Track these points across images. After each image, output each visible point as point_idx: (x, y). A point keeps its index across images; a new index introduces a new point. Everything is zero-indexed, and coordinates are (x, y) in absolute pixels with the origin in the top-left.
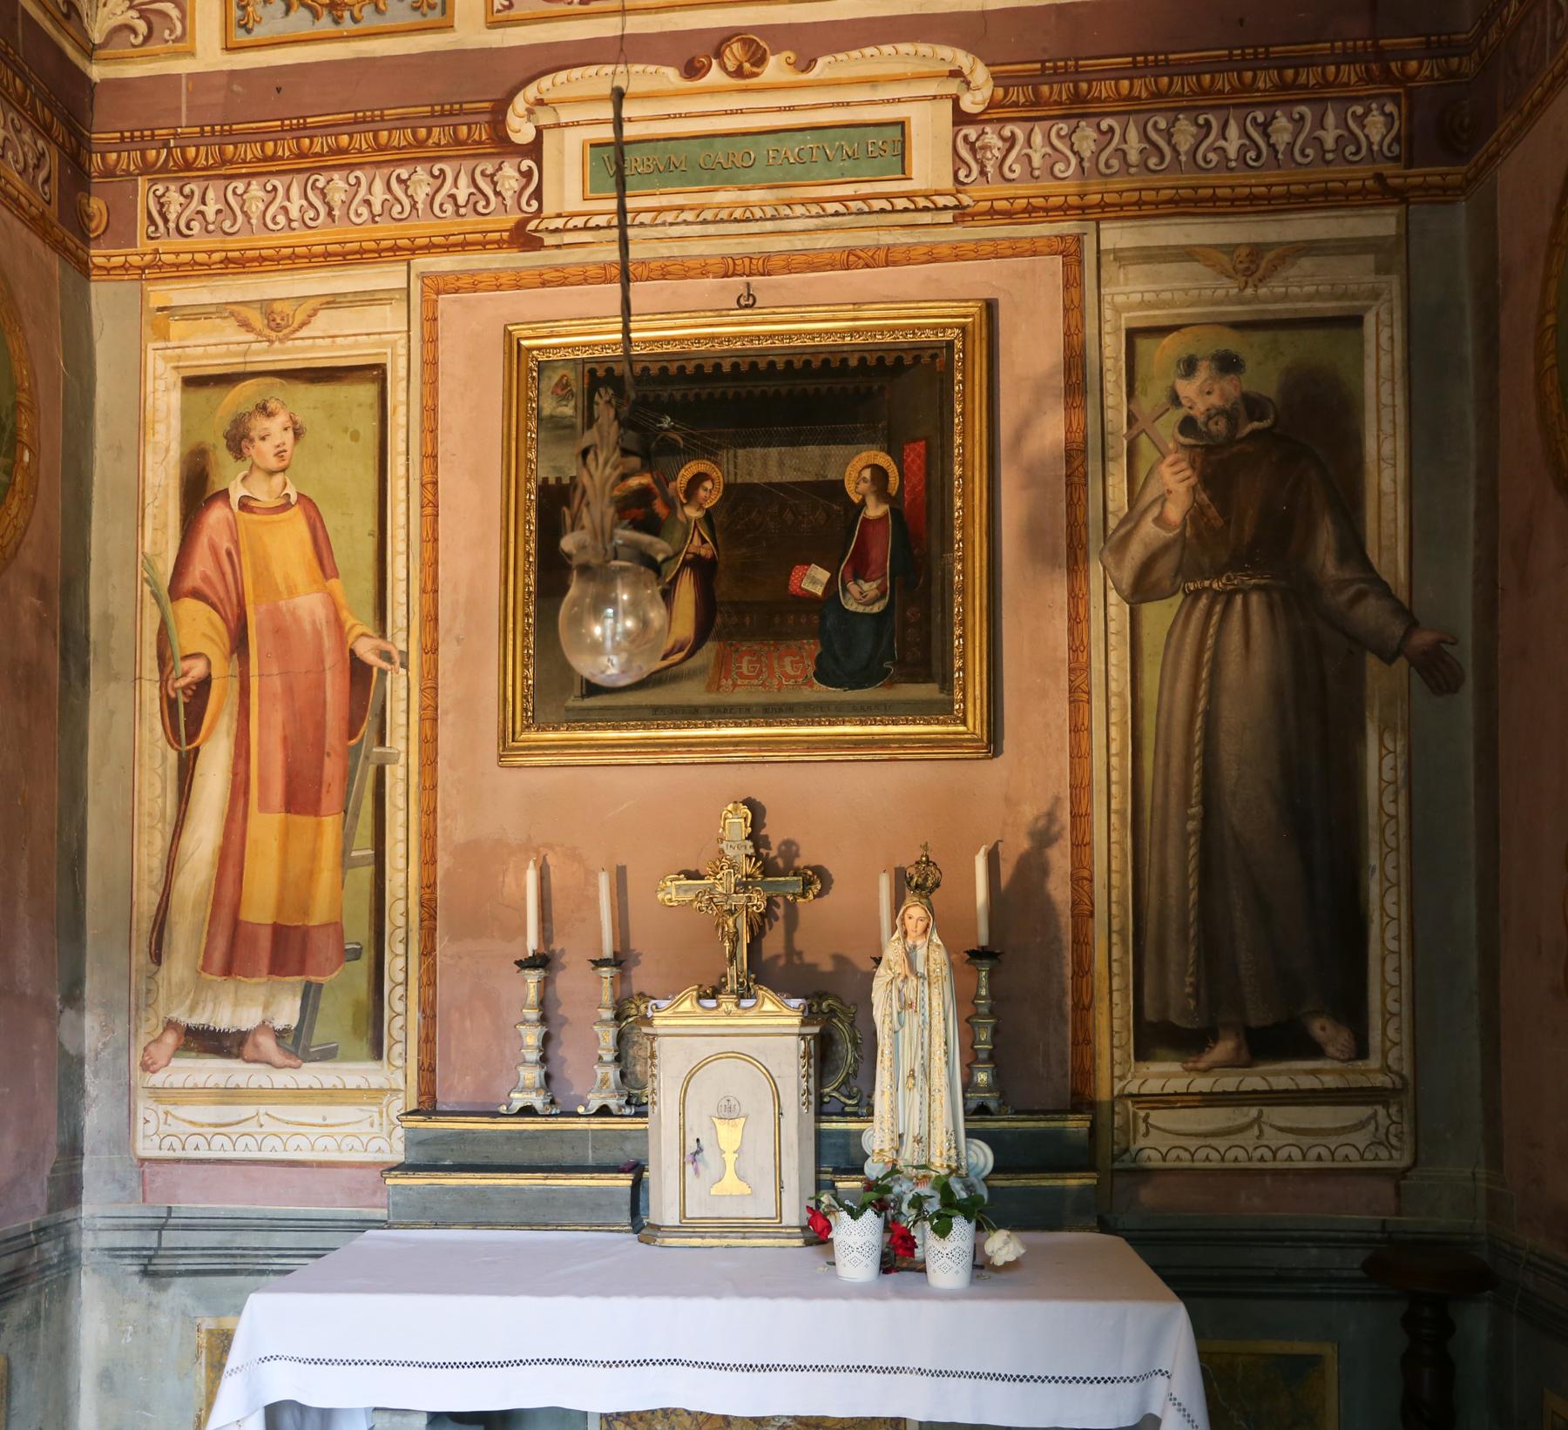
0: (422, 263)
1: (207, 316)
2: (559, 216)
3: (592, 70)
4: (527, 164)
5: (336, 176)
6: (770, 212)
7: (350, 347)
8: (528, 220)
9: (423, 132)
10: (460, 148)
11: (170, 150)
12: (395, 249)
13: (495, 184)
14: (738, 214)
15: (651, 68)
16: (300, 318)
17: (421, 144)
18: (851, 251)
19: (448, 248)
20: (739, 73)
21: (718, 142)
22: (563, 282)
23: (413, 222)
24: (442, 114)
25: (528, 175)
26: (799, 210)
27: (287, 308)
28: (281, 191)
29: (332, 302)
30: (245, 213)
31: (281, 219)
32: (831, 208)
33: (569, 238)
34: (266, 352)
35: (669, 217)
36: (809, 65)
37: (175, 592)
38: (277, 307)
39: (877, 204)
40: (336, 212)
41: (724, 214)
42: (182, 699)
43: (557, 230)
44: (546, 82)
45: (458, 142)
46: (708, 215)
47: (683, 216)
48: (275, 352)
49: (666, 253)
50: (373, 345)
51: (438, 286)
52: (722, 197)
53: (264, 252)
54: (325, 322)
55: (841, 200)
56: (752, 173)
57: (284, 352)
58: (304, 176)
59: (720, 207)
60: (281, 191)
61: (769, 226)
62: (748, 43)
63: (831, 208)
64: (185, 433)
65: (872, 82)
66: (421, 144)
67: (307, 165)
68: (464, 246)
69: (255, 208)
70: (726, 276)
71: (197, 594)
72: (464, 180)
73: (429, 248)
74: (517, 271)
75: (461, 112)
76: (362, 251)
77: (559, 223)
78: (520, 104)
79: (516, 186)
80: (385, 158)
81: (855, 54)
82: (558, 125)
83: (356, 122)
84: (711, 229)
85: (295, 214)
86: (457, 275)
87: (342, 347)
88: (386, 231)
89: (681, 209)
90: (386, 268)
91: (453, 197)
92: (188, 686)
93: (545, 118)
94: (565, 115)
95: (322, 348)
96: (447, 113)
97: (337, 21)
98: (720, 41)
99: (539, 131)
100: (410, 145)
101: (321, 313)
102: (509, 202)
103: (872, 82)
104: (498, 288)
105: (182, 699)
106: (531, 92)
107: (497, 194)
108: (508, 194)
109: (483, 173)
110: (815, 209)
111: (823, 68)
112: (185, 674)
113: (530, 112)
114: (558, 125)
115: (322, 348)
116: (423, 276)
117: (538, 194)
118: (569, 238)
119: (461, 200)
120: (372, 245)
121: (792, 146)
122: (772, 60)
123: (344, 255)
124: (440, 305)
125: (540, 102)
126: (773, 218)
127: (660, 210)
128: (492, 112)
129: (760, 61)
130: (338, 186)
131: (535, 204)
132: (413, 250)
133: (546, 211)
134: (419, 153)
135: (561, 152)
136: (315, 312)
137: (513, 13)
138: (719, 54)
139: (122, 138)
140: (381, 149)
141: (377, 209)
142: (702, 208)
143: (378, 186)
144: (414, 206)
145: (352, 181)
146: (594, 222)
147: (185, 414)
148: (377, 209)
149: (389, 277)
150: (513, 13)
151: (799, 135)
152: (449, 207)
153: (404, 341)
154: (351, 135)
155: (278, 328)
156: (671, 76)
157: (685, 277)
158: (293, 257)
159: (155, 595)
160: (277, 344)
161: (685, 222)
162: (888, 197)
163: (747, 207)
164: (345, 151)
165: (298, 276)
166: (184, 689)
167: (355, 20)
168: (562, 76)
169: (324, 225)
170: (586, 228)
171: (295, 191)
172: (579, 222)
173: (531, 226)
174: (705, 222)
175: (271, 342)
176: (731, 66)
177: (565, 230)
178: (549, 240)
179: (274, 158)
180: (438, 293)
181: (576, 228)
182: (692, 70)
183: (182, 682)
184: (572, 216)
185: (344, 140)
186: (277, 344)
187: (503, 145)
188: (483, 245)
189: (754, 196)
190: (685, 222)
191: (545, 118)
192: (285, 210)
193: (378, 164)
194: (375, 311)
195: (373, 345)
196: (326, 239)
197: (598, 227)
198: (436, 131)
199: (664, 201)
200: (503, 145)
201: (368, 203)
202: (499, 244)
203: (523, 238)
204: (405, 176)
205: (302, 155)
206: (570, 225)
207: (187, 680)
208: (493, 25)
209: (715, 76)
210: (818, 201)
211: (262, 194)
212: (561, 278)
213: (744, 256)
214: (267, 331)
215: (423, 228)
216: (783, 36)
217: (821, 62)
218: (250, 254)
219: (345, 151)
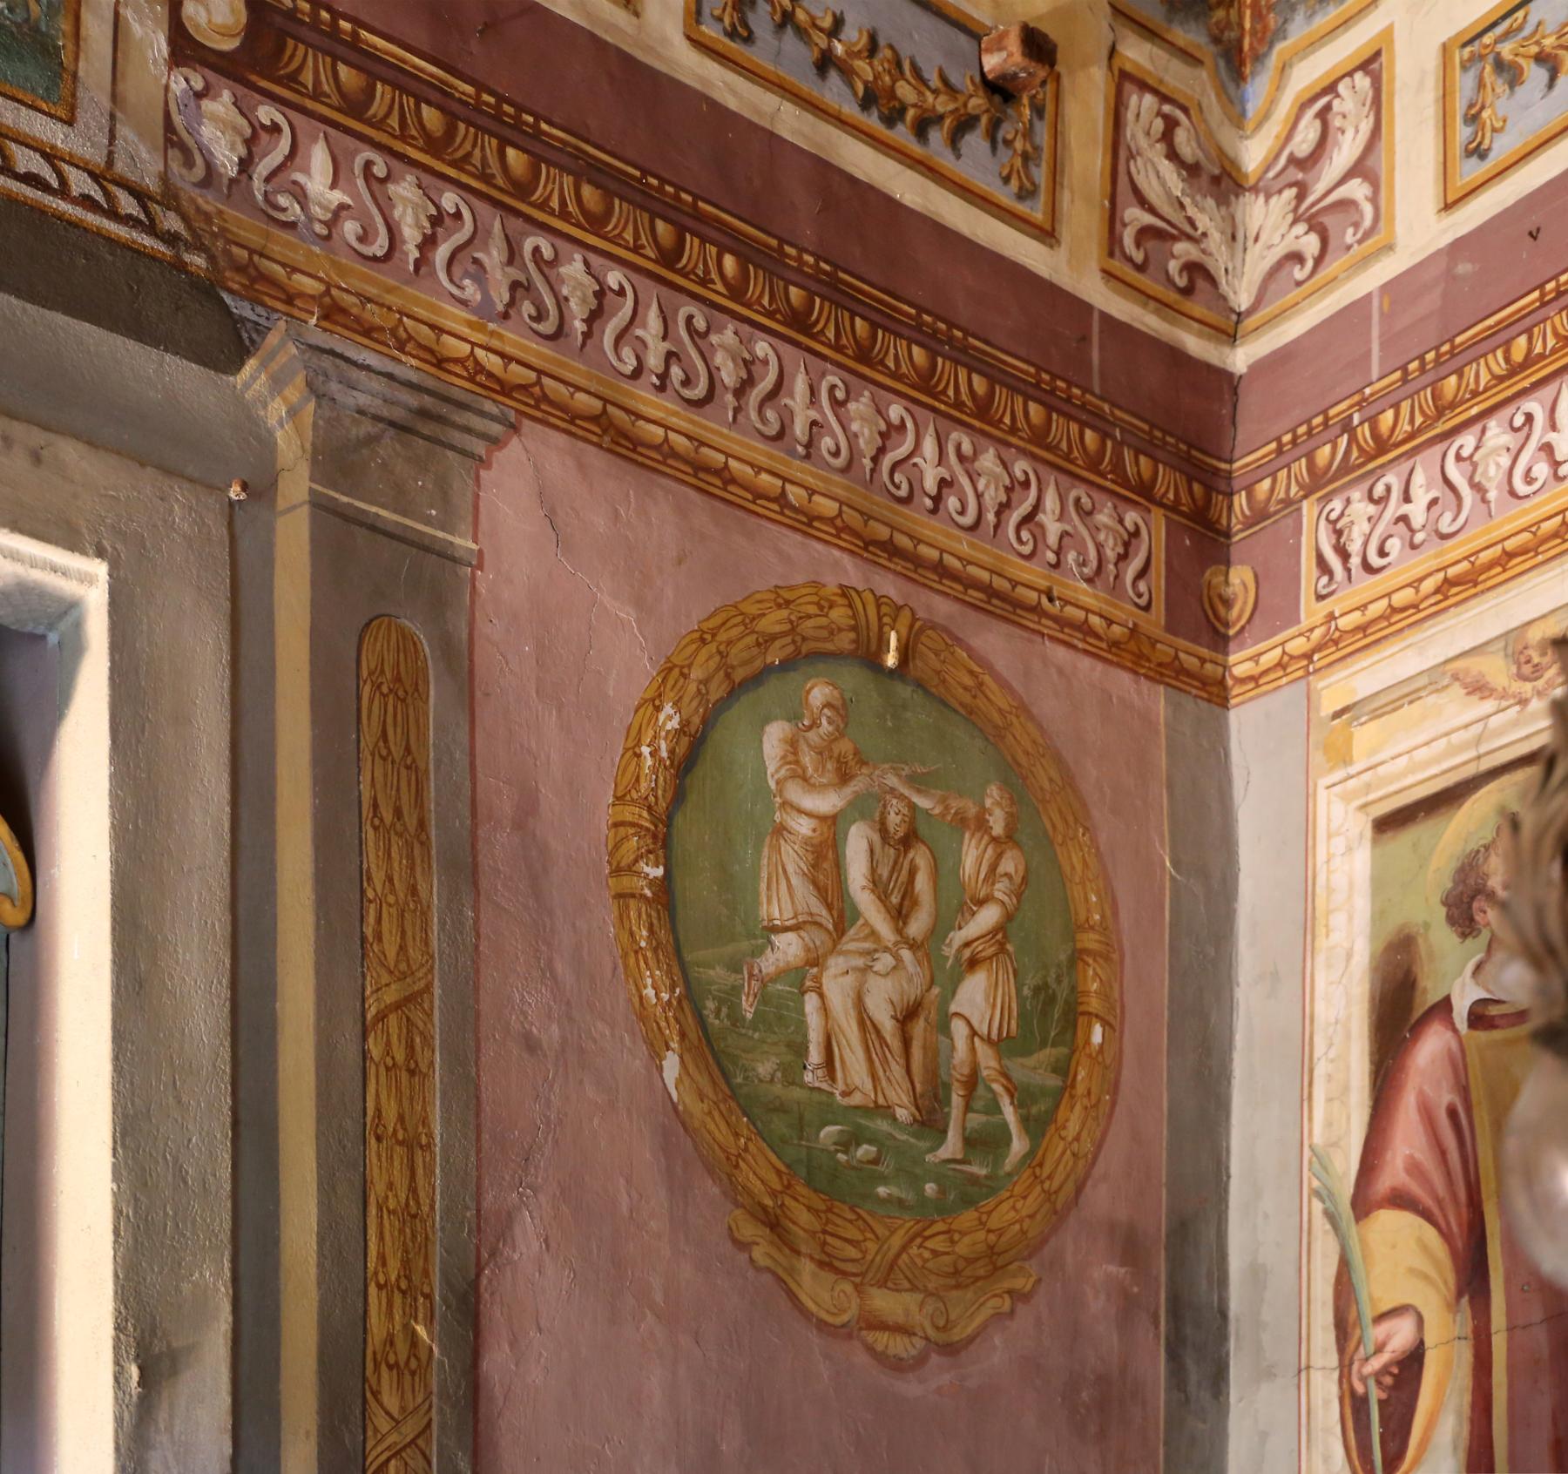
1: (1413, 697)
37: (1363, 1205)
42: (1375, 1395)
53: (1510, 545)
64: (1378, 916)
69: (1493, 472)
71: (1400, 1200)
92: (1385, 1370)
105: (1375, 1395)
112: (1379, 1349)
147: (1378, 884)
159: (1330, 1216)
166: (1378, 1376)
183: (1376, 1364)
207: (1385, 1357)
218: (1485, 556)
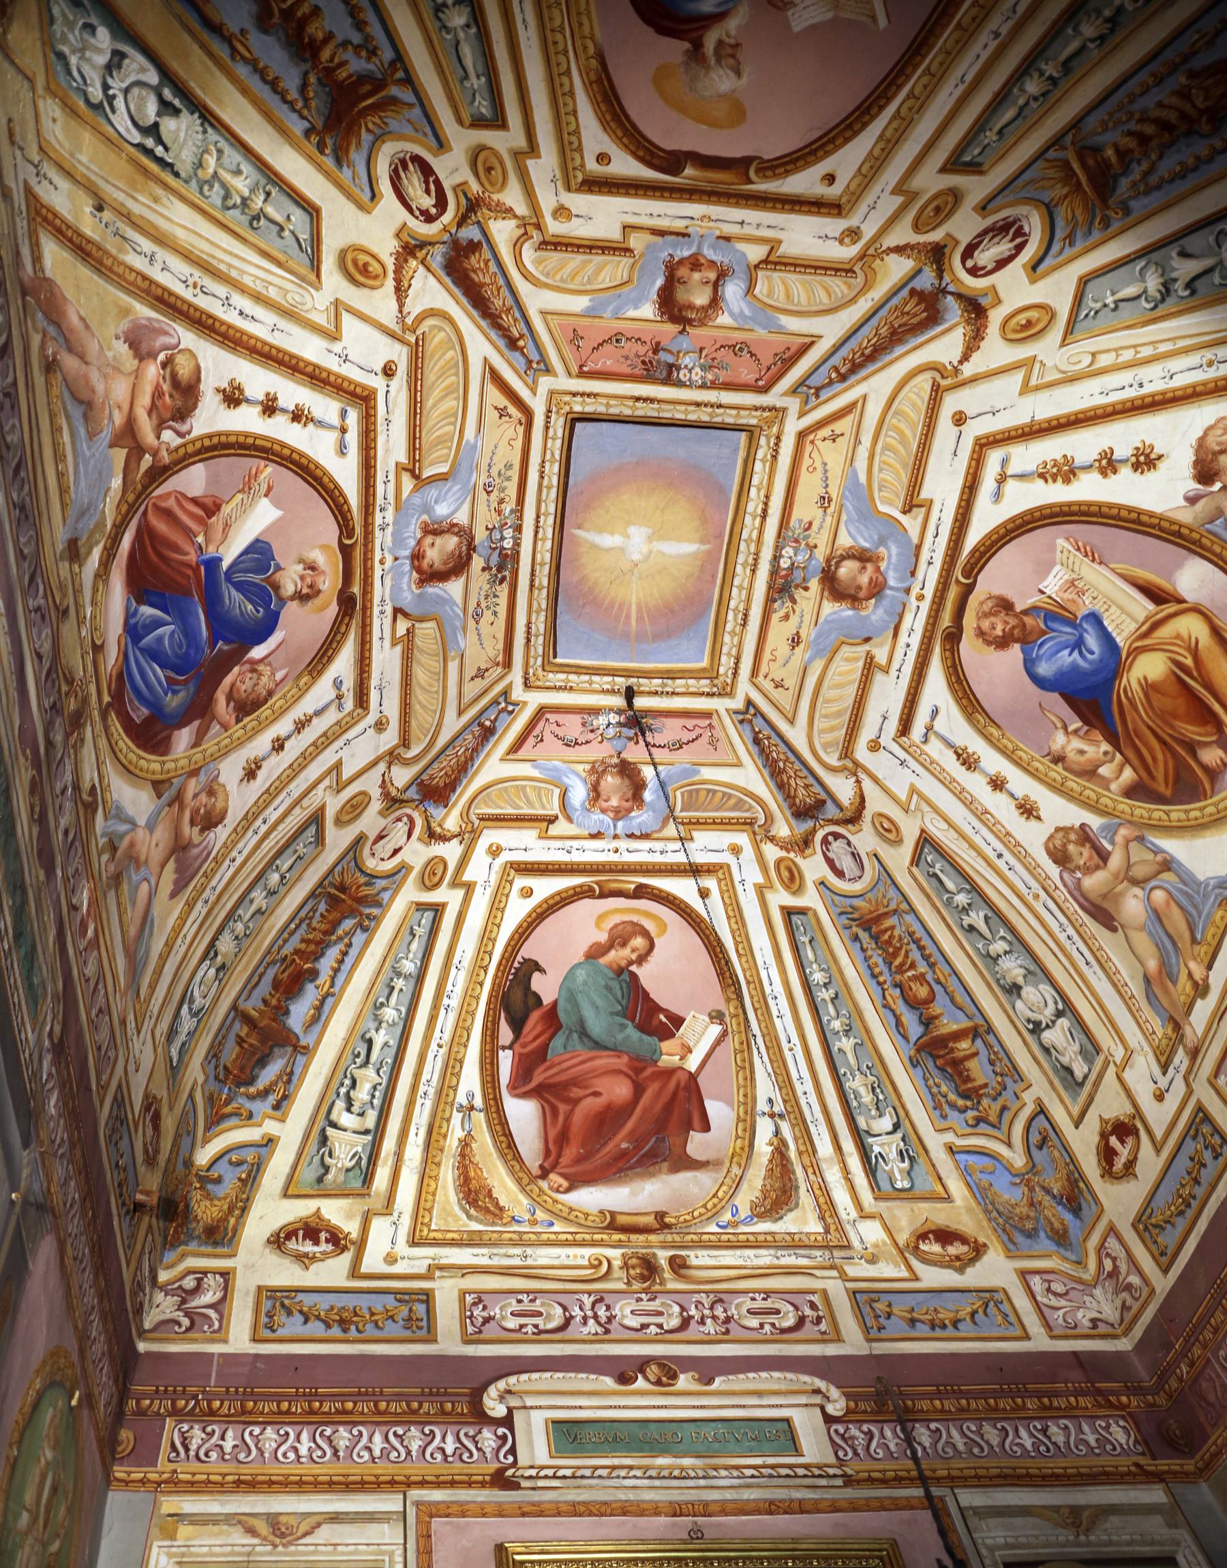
0: (415, 1494)
2: (532, 1467)
3: (548, 1375)
4: (500, 1431)
5: (341, 1429)
6: (701, 1473)
7: (350, 1553)
8: (506, 1469)
9: (415, 1405)
10: (445, 1418)
11: (197, 1402)
12: (392, 1483)
13: (476, 1443)
14: (676, 1473)
15: (593, 1376)
16: (303, 1528)
17: (415, 1412)
18: (771, 1502)
19: (438, 1484)
20: (659, 1383)
21: (652, 1426)
22: (541, 1514)
23: (408, 1464)
24: (431, 1394)
25: (504, 1438)
26: (724, 1473)
27: (293, 1521)
28: (292, 1435)
29: (335, 1518)
30: (259, 1449)
31: (291, 1455)
32: (748, 1472)
33: (541, 1483)
34: (270, 1554)
35: (623, 1473)
36: (710, 1381)
38: (283, 1519)
39: (784, 1471)
40: (341, 1454)
41: (665, 1473)
43: (531, 1477)
44: (512, 1380)
45: (443, 1412)
46: (653, 1473)
47: (632, 1473)
48: (281, 1554)
49: (623, 1497)
50: (371, 1553)
51: (429, 1512)
52: (660, 1461)
54: (325, 1533)
55: (755, 1467)
56: (681, 1447)
57: (286, 1554)
58: (313, 1427)
59: (661, 1468)
60: (292, 1435)
61: (702, 1482)
62: (662, 1366)
63: (748, 1472)
65: (759, 1394)
66: (415, 1412)
67: (314, 1419)
68: (453, 1484)
70: (675, 1515)
72: (450, 1439)
73: (423, 1484)
74: (500, 1504)
75: (446, 1394)
76: (363, 1483)
77: (533, 1472)
78: (493, 1391)
79: (494, 1445)
80: (381, 1419)
81: (741, 1376)
82: (525, 1407)
83: (359, 1394)
84: (657, 1483)
85: (303, 1451)
86: (448, 1504)
87: (343, 1554)
88: (384, 1470)
89: (631, 1468)
90: (384, 1496)
91: (443, 1450)
93: (514, 1402)
94: (529, 1402)
95: (323, 1553)
96: (433, 1394)
97: (345, 1331)
98: (642, 1364)
99: (510, 1410)
100: (404, 1413)
101: (324, 1527)
102: (489, 1455)
103: (759, 1394)
104: (484, 1515)
106: (501, 1385)
107: (479, 1449)
108: (488, 1451)
109: (466, 1435)
110: (735, 1473)
111: (719, 1382)
113: (501, 1398)
114: (525, 1407)
115: (323, 1553)
116: (418, 1504)
117: (513, 1451)
118: (541, 1483)
119: (449, 1451)
120: (373, 1479)
121: (709, 1431)
122: (682, 1377)
123: (347, 1484)
124: (433, 1526)
125: (509, 1392)
126: (704, 1477)
127: (614, 1468)
128: (470, 1395)
129: (674, 1377)
130: (343, 1436)
131: (511, 1459)
132: (409, 1484)
133: (521, 1463)
134: (411, 1418)
135: (529, 1425)
136: (319, 1525)
137: (482, 1336)
138: (643, 1372)
139: (157, 1391)
140: (379, 1412)
141: (377, 1453)
142: (646, 1468)
143: (378, 1438)
144: (409, 1453)
145: (355, 1432)
146: (561, 1473)
148: (377, 1453)
149: (390, 1503)
150: (482, 1336)
151: (713, 1425)
152: (439, 1457)
153: (400, 1551)
154: (355, 1403)
155: (283, 1535)
156: (608, 1382)
157: (642, 1515)
158: (300, 1483)
160: (280, 1548)
161: (635, 1477)
162: (790, 1467)
163: (682, 1469)
164: (351, 1413)
165: (304, 1497)
167: (359, 1331)
168: (524, 1377)
169: (329, 1462)
170: (555, 1477)
171: (305, 1436)
172: (550, 1472)
173: (510, 1472)
174: (650, 1477)
175: (275, 1546)
176: (652, 1378)
177: (537, 1477)
178: (524, 1484)
179: (288, 1412)
180: (431, 1516)
181: (546, 1477)
182: (624, 1379)
184: (542, 1468)
185: (350, 1405)
186: (280, 1548)
187: (481, 1417)
188: (469, 1484)
189: (687, 1462)
190: (635, 1477)
191: (514, 1402)
192: (296, 1450)
193: (378, 1423)
194: (375, 1527)
195: (371, 1553)
196: (331, 1472)
197: (564, 1477)
198: (426, 1405)
199: (616, 1462)
200: (481, 1417)
201: (369, 1449)
202: (483, 1484)
203: (501, 1480)
204: (400, 1432)
205: (312, 1412)
206: (542, 1473)
208: (467, 1342)
209: (641, 1383)
210: (737, 1467)
211: (275, 1436)
212: (539, 1511)
213: (687, 1503)
214: (271, 1537)
215: (415, 1470)
216: (688, 1363)
217: (718, 1380)
219: (351, 1413)
